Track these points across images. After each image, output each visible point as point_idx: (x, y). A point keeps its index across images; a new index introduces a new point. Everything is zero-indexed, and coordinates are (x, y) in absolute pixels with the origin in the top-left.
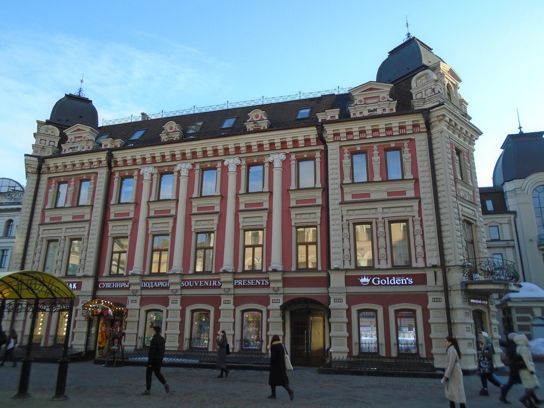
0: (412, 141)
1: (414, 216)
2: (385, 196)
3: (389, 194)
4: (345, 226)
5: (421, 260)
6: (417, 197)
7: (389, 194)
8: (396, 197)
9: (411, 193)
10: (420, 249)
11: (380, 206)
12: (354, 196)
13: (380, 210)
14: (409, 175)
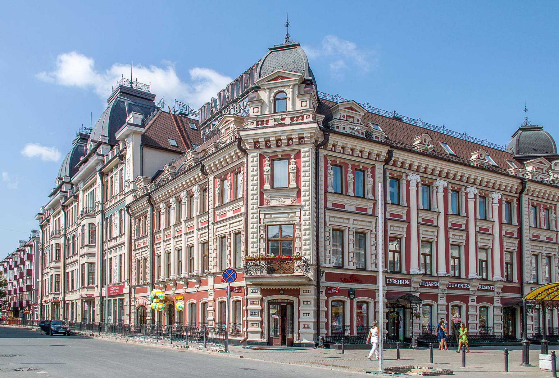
0: (373, 168)
1: (371, 231)
2: (354, 210)
3: (357, 208)
4: (327, 230)
5: (374, 266)
6: (374, 215)
7: (357, 208)
8: (361, 211)
9: (370, 211)
10: (374, 257)
11: (352, 217)
12: (334, 205)
13: (352, 221)
14: (370, 196)
